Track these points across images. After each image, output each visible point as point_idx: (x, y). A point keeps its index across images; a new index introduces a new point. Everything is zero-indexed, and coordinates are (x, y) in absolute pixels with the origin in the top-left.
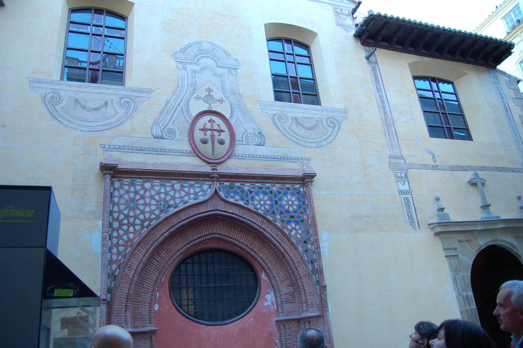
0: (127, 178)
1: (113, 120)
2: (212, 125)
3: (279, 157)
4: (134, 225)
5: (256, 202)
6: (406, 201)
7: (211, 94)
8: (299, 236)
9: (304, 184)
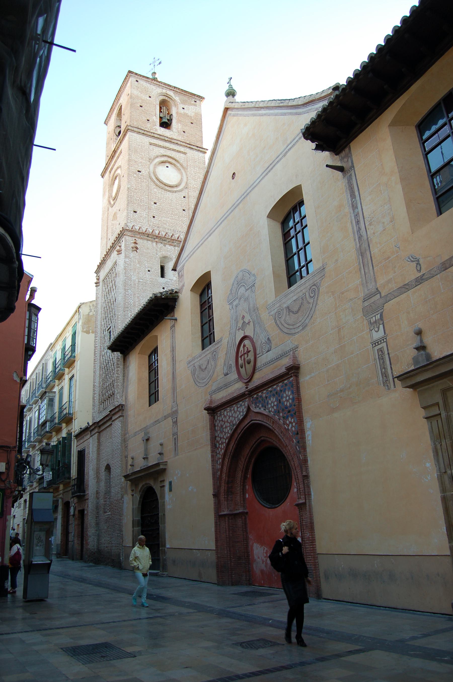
6: (380, 353)
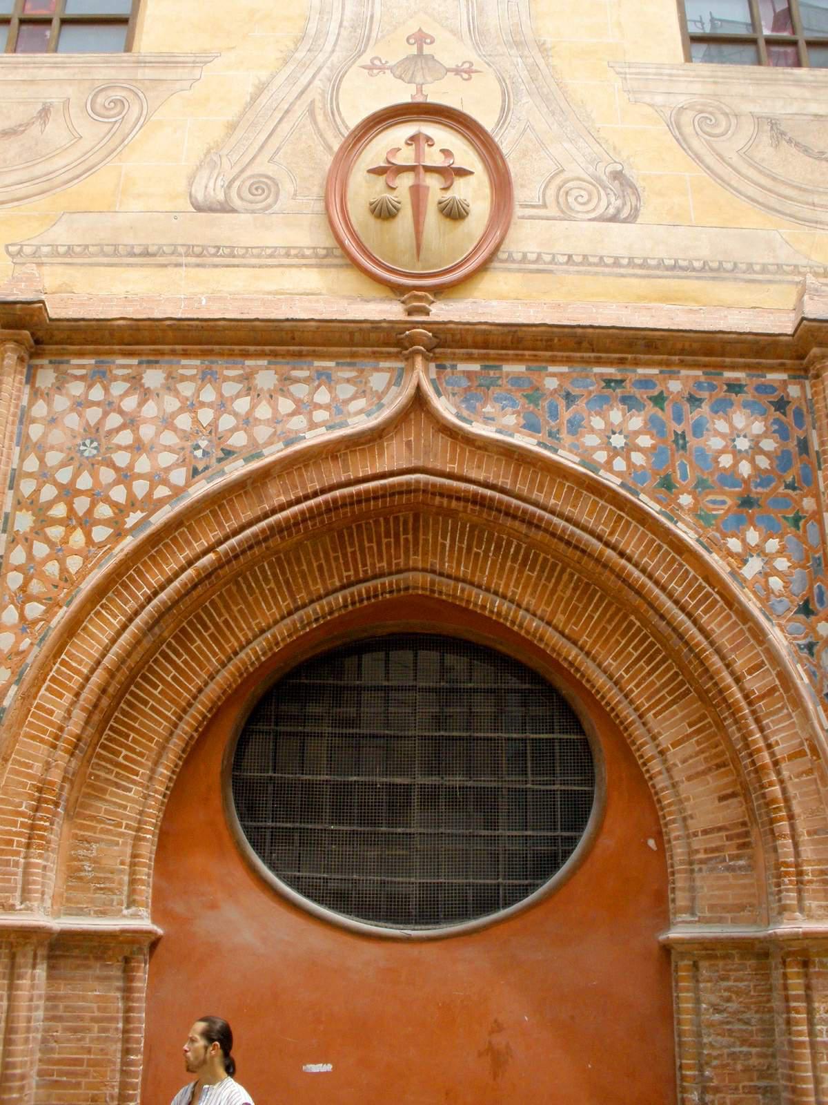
0: (81, 354)
1: (59, 162)
2: (419, 154)
3: (697, 264)
4: (87, 522)
5: (591, 440)
7: (427, 50)
8: (776, 583)
9: (806, 370)
